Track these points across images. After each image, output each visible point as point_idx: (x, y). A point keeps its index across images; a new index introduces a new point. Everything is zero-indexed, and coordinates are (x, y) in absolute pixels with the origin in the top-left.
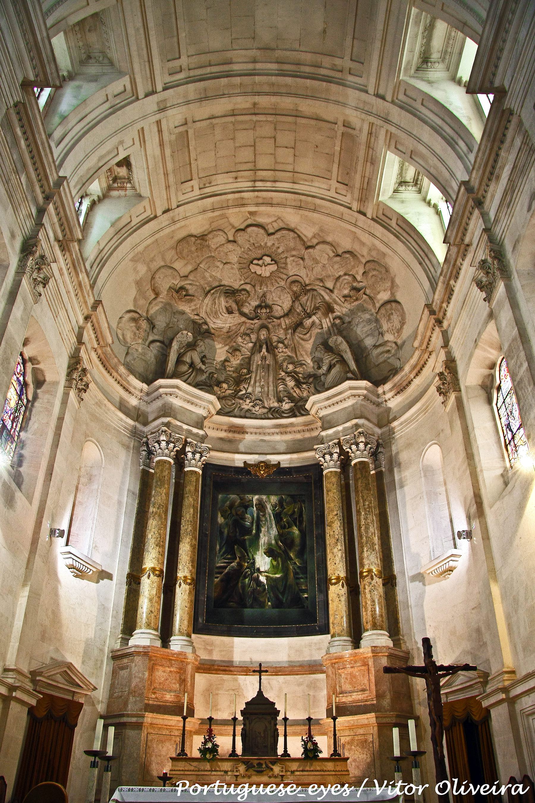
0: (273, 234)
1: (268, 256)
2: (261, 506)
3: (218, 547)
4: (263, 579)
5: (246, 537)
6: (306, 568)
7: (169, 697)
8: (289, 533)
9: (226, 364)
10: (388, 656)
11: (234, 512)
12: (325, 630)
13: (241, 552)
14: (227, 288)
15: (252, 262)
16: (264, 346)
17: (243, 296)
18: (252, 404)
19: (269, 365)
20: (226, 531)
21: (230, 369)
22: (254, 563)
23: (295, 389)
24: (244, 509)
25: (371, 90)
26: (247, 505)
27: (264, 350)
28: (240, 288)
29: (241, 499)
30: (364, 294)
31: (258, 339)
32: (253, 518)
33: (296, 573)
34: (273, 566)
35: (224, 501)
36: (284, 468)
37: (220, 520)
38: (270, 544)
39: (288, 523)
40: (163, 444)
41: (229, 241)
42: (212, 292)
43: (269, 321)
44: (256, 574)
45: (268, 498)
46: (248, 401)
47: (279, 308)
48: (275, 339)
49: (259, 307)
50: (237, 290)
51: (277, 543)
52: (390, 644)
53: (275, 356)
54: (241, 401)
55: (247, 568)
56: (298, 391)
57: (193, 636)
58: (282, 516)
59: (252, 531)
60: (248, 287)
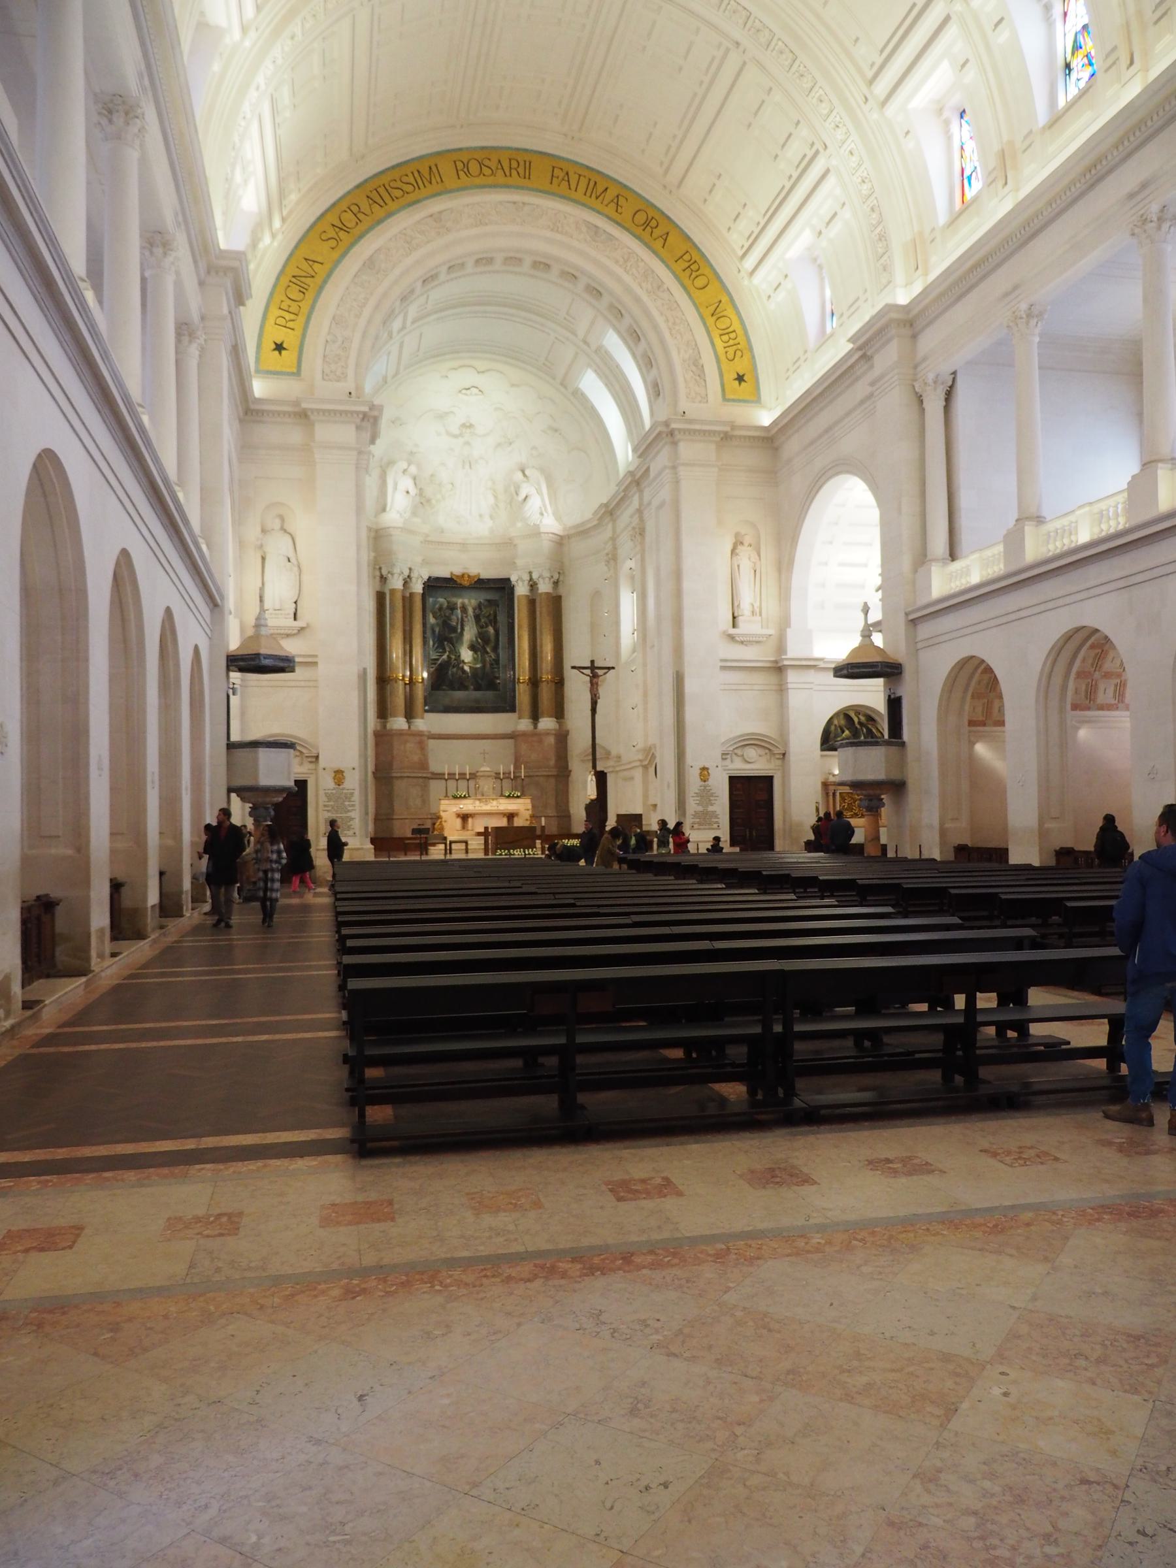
0: (483, 372)
1: (477, 388)
2: (464, 609)
3: (431, 643)
4: (467, 668)
5: (453, 635)
6: (499, 660)
7: (416, 758)
8: (487, 631)
10: (555, 735)
11: (443, 615)
12: (512, 709)
13: (450, 648)
20: (437, 630)
22: (459, 656)
24: (448, 612)
25: (581, 334)
26: (452, 608)
29: (448, 602)
32: (458, 619)
33: (491, 664)
34: (474, 658)
35: (435, 603)
36: (482, 580)
37: (432, 620)
38: (472, 641)
39: (486, 624)
40: (396, 576)
41: (442, 377)
44: (461, 665)
45: (469, 601)
49: (464, 425)
50: (447, 413)
51: (477, 640)
52: (557, 726)
55: (455, 660)
57: (426, 714)
58: (481, 617)
59: (457, 629)
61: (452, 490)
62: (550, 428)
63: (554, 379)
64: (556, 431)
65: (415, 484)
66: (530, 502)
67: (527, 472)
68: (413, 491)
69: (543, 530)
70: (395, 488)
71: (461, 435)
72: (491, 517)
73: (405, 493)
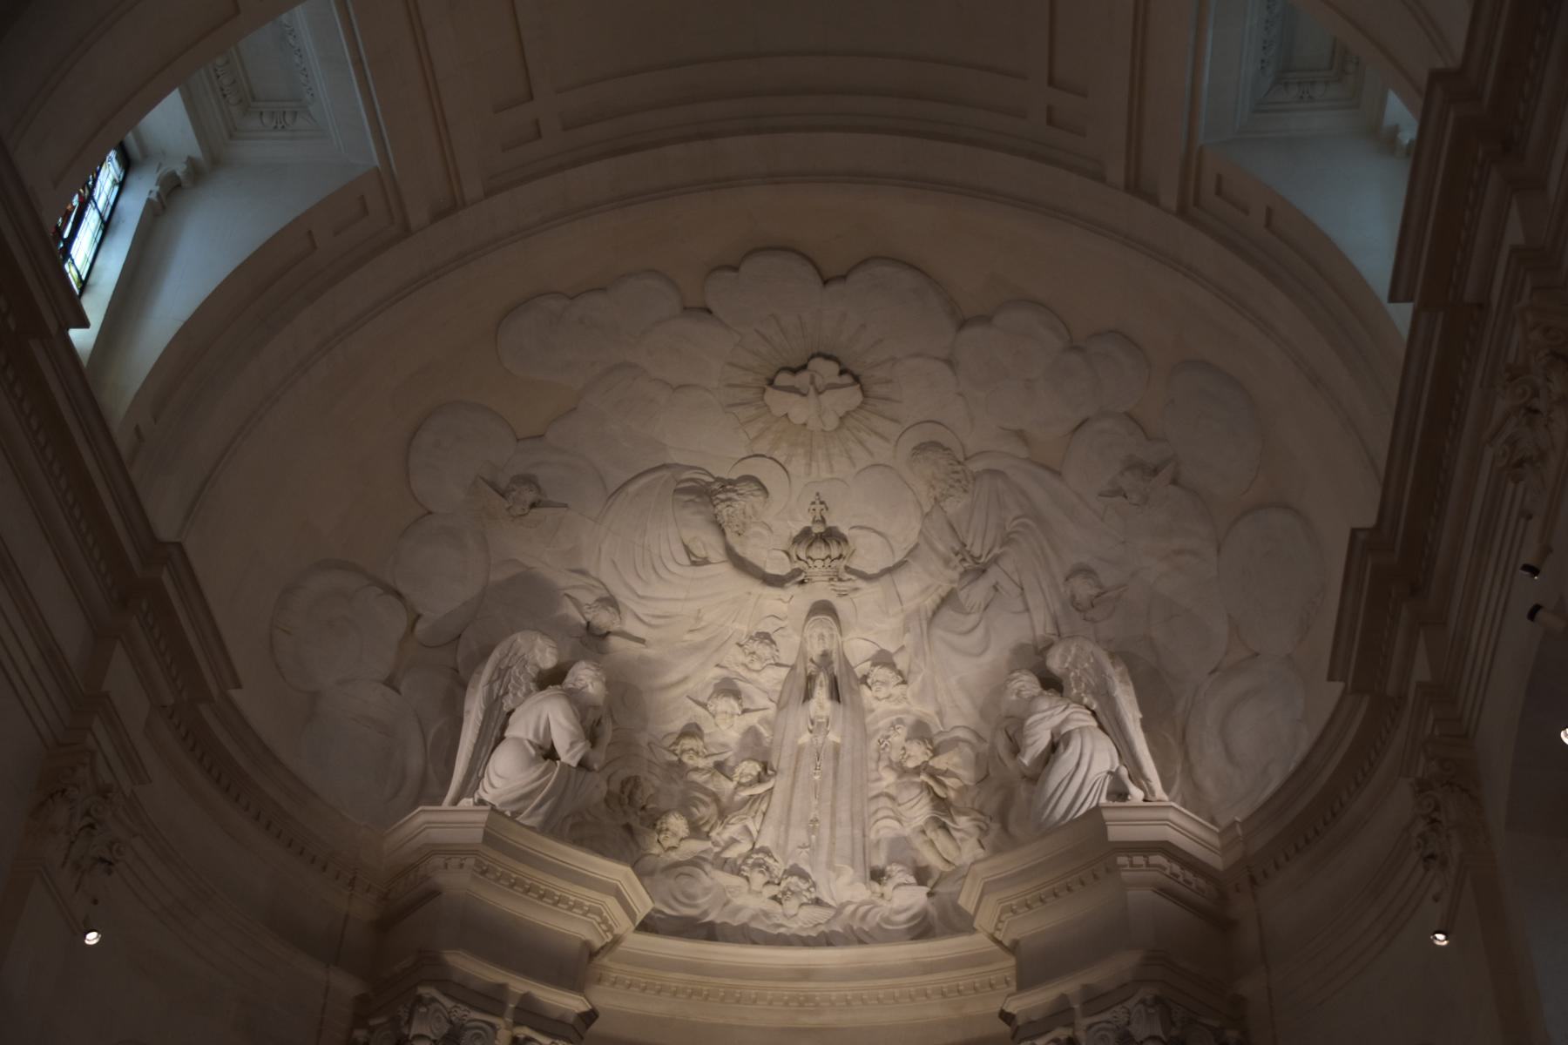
0: (844, 277)
1: (828, 357)
9: (688, 743)
14: (687, 475)
15: (771, 382)
16: (822, 679)
17: (744, 503)
18: (774, 890)
19: (837, 750)
21: (701, 763)
23: (931, 834)
27: (821, 693)
28: (734, 476)
30: (1174, 482)
31: (802, 653)
42: (632, 489)
43: (842, 586)
46: (758, 879)
47: (876, 540)
48: (858, 648)
49: (805, 537)
50: (727, 485)
53: (860, 712)
54: (736, 881)
56: (940, 839)
60: (761, 469)
61: (759, 780)
62: (1132, 465)
63: (1100, 177)
64: (1155, 471)
65: (592, 734)
66: (1068, 758)
67: (1055, 663)
68: (569, 752)
69: (1116, 833)
70: (494, 733)
71: (796, 578)
72: (922, 875)
73: (533, 752)
